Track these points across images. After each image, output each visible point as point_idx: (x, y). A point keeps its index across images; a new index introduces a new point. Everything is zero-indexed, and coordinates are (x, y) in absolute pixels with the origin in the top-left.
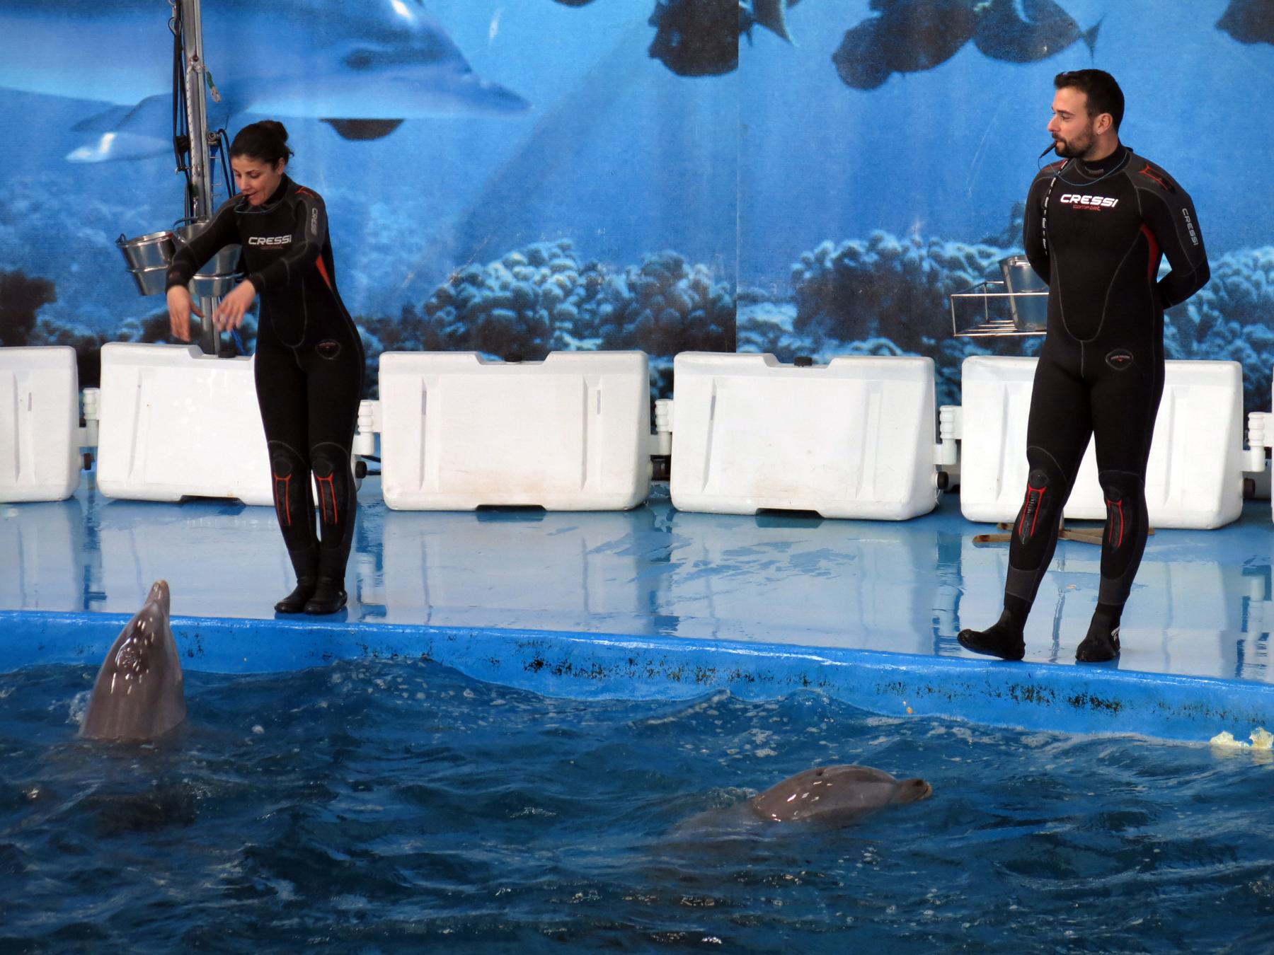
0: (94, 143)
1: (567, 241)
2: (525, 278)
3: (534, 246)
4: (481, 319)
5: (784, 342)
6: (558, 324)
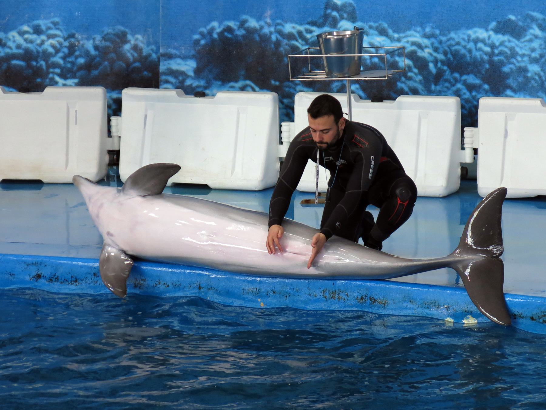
1: (57, 19)
2: (31, 42)
3: (36, 22)
4: (5, 66)
5: (188, 82)
6: (51, 70)
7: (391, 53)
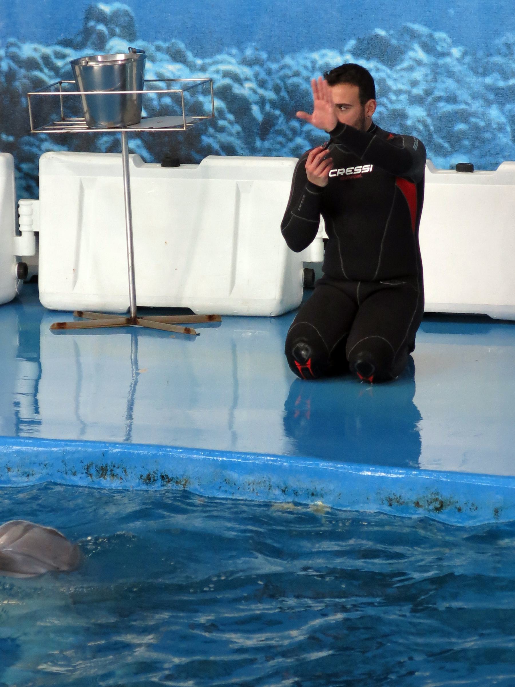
7: (192, 88)
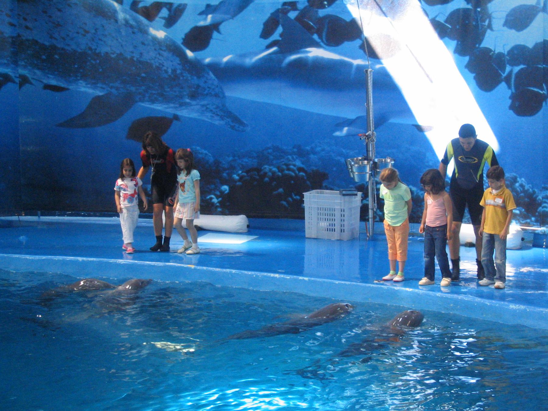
0: (341, 130)
